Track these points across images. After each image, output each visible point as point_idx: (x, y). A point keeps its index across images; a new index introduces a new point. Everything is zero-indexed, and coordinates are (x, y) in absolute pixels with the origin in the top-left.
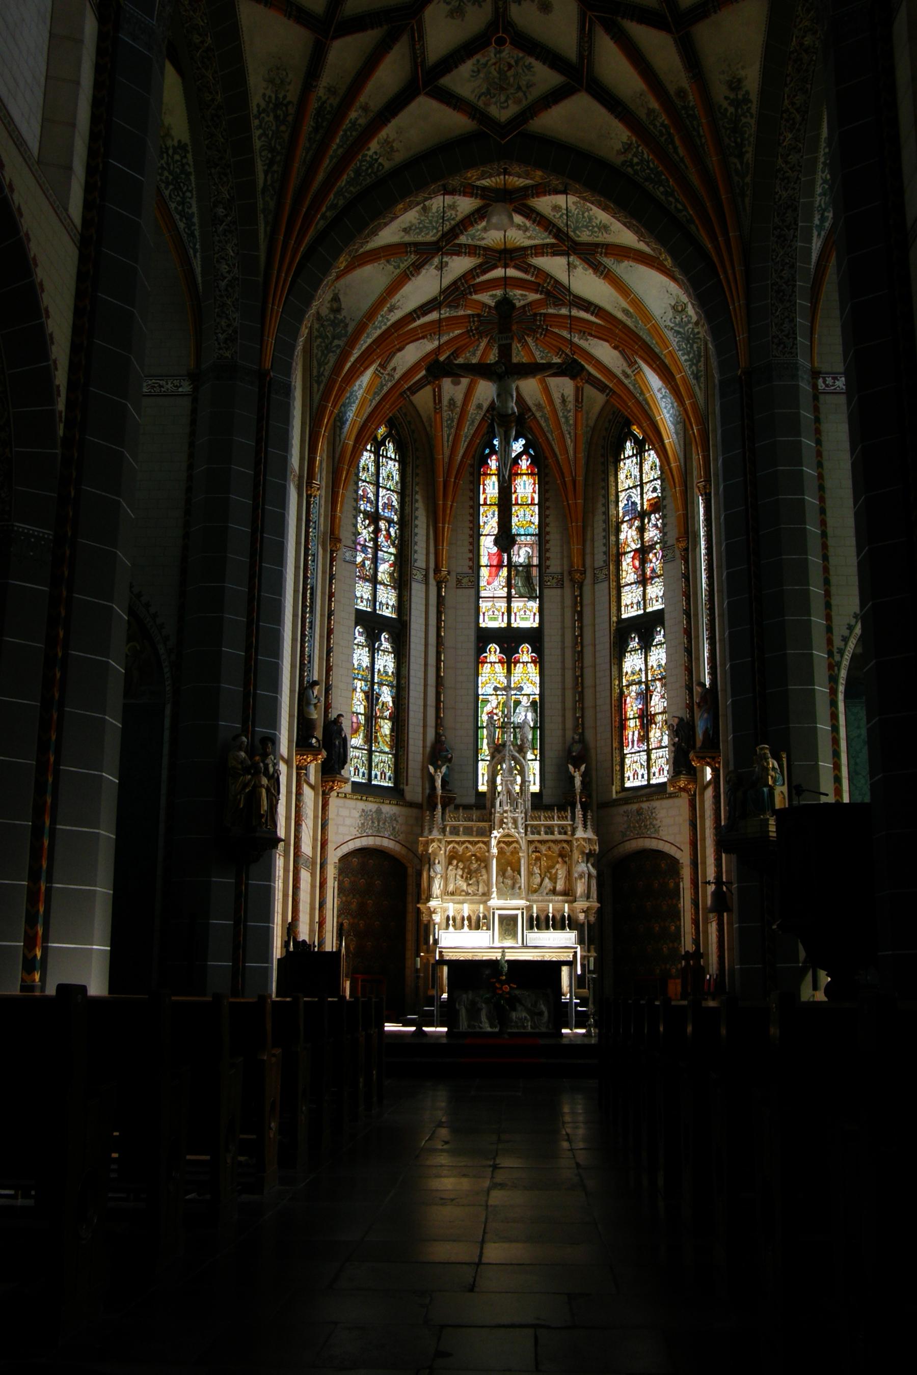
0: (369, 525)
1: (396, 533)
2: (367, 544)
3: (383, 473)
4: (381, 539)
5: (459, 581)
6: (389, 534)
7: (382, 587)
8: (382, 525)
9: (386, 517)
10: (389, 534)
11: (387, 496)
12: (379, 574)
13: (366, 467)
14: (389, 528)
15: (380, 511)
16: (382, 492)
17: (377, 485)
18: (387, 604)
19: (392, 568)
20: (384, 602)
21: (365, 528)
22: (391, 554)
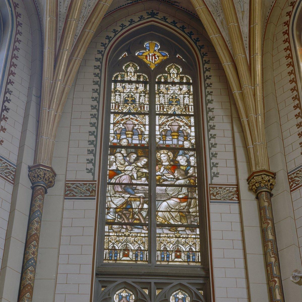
0: (137, 160)
1: (188, 161)
2: (134, 182)
3: (160, 100)
4: (161, 171)
5: (291, 180)
6: (175, 166)
7: (166, 231)
8: (163, 156)
9: (168, 145)
10: (175, 166)
11: (168, 123)
12: (160, 214)
13: (130, 99)
14: (175, 156)
15: (158, 140)
16: (158, 120)
17: (152, 114)
18: (179, 251)
19: (185, 204)
20: (170, 247)
21: (130, 164)
22: (181, 186)
